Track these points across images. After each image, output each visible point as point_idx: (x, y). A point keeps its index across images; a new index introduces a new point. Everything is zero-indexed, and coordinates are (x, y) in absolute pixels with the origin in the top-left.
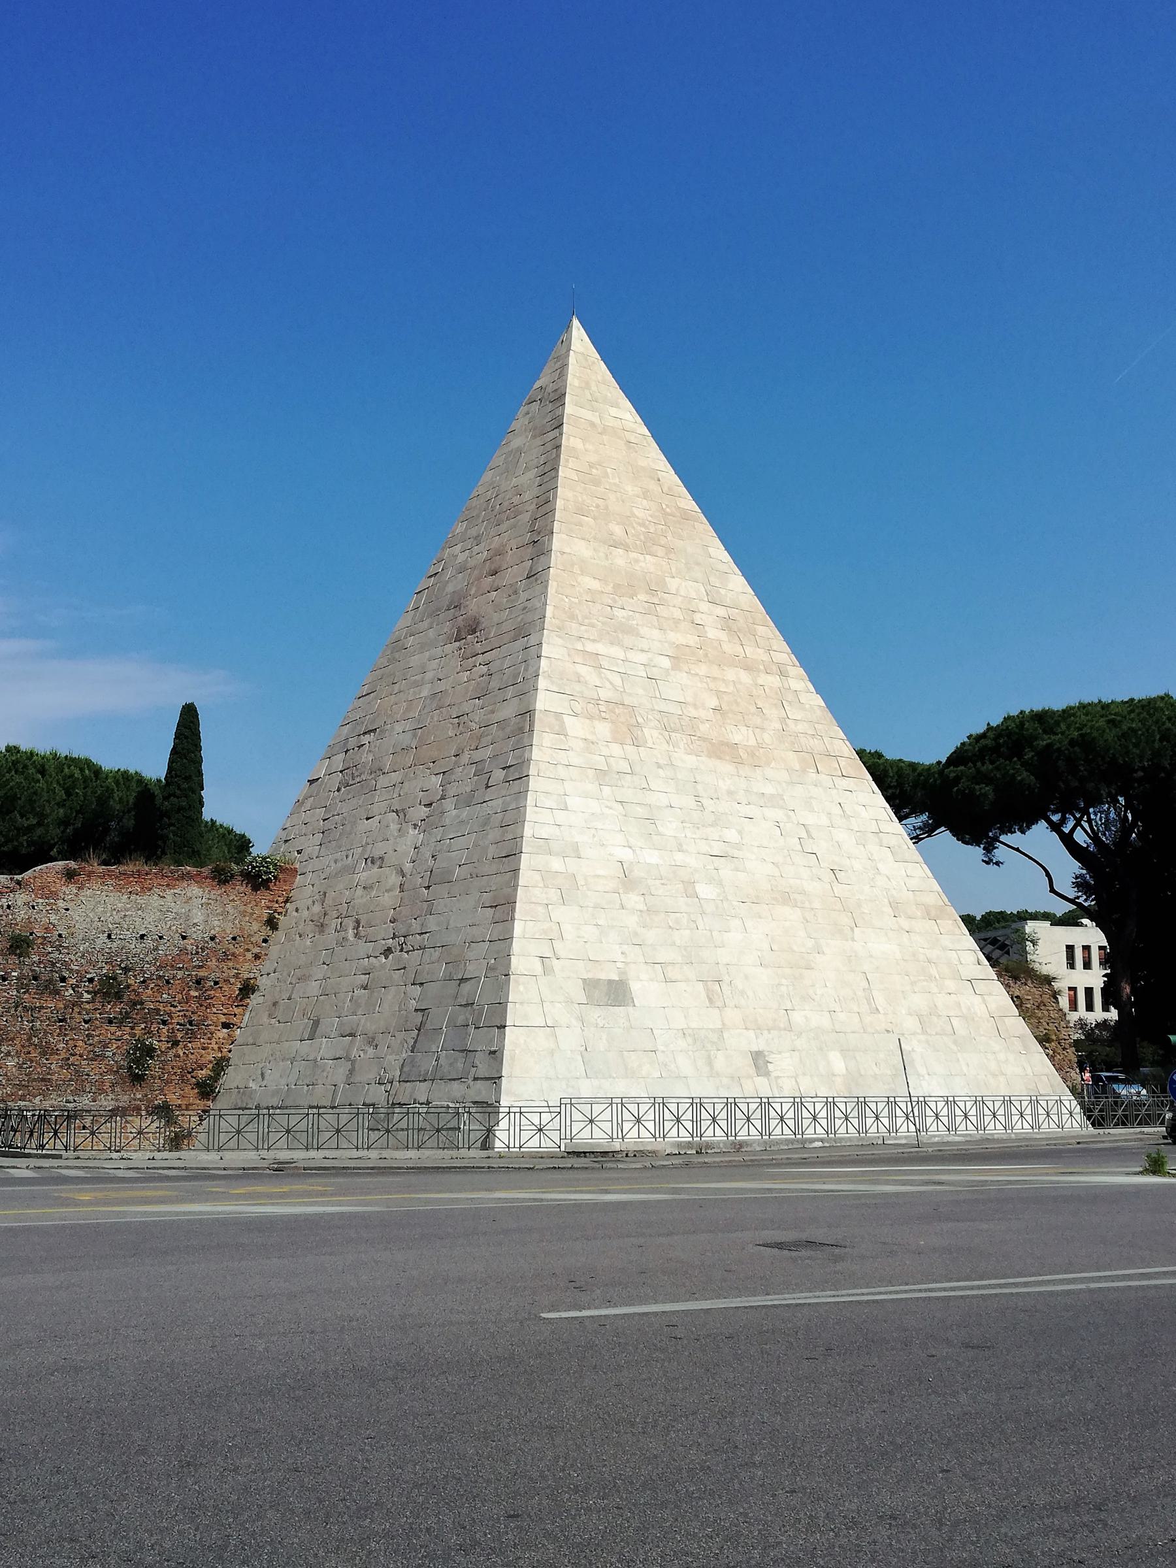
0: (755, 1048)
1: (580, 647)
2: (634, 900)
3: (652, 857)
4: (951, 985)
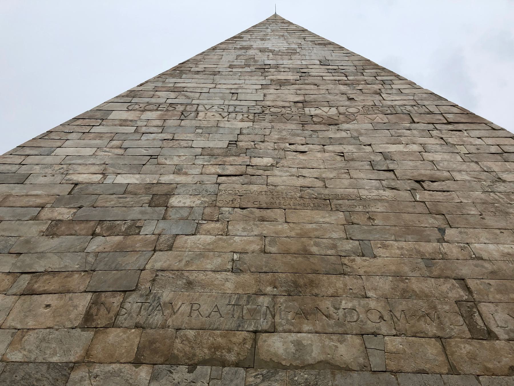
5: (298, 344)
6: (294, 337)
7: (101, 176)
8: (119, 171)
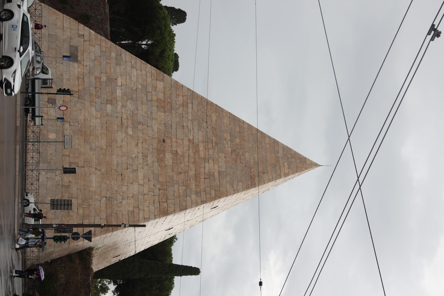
0: (57, 101)
1: (189, 101)
2: (104, 78)
3: (119, 92)
4: (81, 211)
5: (67, 129)
6: (69, 129)
7: (120, 85)
8: (123, 90)
